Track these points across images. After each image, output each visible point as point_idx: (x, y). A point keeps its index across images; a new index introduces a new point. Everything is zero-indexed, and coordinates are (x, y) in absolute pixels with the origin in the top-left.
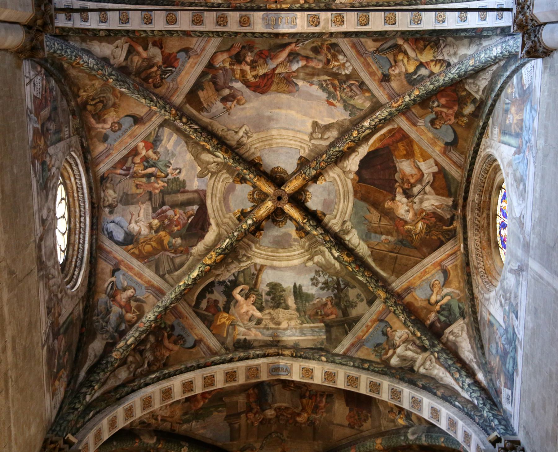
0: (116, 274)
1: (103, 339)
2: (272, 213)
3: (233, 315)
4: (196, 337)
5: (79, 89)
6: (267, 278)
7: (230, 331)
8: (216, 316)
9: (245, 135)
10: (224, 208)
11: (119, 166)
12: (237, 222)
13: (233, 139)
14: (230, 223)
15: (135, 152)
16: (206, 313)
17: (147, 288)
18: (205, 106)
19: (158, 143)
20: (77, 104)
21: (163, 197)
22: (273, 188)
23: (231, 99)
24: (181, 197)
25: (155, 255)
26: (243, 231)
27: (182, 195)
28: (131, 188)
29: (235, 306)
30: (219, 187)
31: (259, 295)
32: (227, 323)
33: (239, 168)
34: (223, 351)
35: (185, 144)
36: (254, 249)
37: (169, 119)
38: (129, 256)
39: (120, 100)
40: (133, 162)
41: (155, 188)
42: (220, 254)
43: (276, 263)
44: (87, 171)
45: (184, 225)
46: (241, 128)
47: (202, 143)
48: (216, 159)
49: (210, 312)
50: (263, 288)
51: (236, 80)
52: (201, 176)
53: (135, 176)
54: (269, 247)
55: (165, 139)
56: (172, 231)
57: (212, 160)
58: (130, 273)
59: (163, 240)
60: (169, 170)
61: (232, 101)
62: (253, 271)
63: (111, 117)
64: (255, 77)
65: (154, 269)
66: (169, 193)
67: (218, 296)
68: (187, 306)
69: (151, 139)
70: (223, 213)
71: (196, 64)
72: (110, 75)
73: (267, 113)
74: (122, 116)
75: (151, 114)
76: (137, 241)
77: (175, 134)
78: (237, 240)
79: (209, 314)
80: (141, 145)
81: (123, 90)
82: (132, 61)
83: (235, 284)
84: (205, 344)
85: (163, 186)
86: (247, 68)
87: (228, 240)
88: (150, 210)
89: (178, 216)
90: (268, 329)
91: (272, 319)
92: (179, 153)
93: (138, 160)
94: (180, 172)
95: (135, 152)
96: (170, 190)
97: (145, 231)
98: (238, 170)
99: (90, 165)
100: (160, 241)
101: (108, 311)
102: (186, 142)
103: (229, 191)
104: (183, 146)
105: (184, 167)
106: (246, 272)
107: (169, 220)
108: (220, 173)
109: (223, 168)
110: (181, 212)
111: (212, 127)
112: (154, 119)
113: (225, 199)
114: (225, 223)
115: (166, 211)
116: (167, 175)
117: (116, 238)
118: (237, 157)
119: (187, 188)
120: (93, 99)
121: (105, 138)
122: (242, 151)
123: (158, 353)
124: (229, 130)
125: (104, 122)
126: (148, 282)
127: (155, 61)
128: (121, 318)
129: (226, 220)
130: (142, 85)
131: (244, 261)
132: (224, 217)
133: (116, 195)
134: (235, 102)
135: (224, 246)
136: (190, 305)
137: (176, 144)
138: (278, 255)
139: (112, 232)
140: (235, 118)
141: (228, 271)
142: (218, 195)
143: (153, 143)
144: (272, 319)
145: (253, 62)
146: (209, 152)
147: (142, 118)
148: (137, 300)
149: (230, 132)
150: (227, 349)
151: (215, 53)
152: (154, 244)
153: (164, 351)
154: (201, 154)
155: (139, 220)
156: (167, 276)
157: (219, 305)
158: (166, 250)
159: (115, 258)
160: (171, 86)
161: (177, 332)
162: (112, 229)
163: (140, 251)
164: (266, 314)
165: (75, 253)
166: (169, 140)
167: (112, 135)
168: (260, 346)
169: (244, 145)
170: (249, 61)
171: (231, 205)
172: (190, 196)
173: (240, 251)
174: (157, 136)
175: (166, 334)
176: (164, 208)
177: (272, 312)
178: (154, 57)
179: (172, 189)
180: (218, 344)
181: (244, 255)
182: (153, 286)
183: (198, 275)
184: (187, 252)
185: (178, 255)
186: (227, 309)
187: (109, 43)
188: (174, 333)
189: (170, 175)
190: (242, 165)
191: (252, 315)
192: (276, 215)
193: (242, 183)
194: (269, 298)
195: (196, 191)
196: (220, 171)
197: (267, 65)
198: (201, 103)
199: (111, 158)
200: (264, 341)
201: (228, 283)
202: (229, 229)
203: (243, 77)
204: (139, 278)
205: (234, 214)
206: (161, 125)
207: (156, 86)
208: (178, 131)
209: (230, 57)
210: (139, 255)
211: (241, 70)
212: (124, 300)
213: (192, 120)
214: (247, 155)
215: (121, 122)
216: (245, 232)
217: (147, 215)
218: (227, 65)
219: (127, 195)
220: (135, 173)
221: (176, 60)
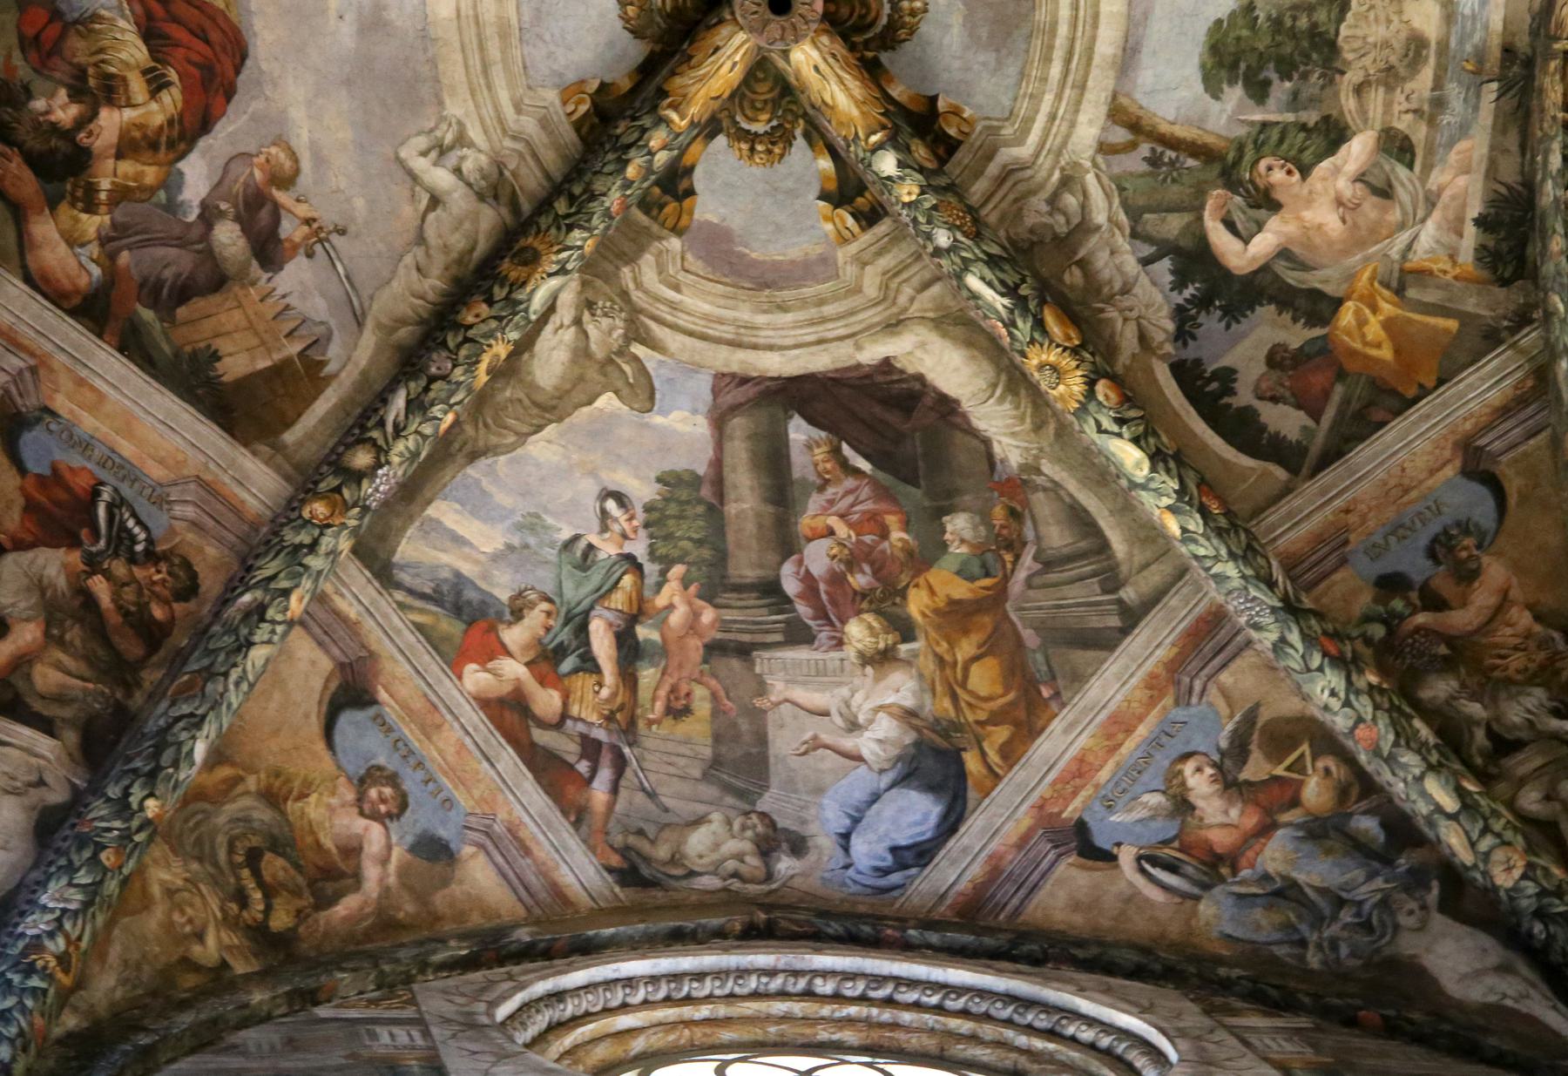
0: (1102, 841)
2: (852, 48)
3: (1351, 277)
4: (1449, 472)
5: (187, 964)
6: (1176, 92)
7: (1431, 296)
8: (1352, 366)
9: (452, 159)
10: (807, 291)
11: (571, 790)
12: (883, 227)
13: (467, 224)
14: (887, 262)
15: (509, 713)
16: (1329, 414)
17: (1183, 700)
18: (294, 349)
19: (470, 594)
20: (264, 976)
21: (739, 588)
22: (725, 31)
23: (264, 215)
24: (745, 499)
25: (1019, 642)
26: (930, 200)
27: (731, 495)
28: (687, 742)
29: (1305, 267)
30: (707, 308)
31: (1263, 138)
32: (1387, 309)
33: (613, 200)
34: (1530, 338)
35: (483, 463)
36: (1024, 152)
37: (355, 532)
38: (1019, 775)
39: (252, 770)
40: (558, 725)
41: (693, 625)
42: (1039, 324)
43: (1107, 43)
44: (588, 949)
45: (882, 493)
46: (413, 177)
47: (482, 376)
48: (565, 314)
49: (1326, 395)
50: (1226, 115)
51: (171, 183)
52: (644, 394)
53: (625, 718)
54: (1022, 75)
55: (449, 560)
56: (910, 553)
57: (569, 335)
58: (1104, 775)
59: (953, 603)
60: (608, 549)
61: (276, 209)
62: (1134, 163)
63: (331, 816)
64: (157, 85)
66: (721, 558)
67: (1248, 347)
68: (1284, 507)
69: (451, 627)
70: (836, 298)
71: (81, 382)
73: (345, 35)
74: (327, 763)
75: (324, 622)
76: (947, 729)
77: (431, 511)
78: (977, 237)
79: (1339, 391)
80: (475, 677)
81: (200, 750)
82: (60, 699)
83: (1194, 260)
84: (1487, 428)
85: (685, 583)
86: (110, 122)
87: (973, 282)
88: (801, 654)
89: (833, 521)
90: (1439, 103)
91: (1390, 77)
92: (525, 494)
93: (547, 701)
94: (620, 498)
96: (706, 553)
97: (901, 689)
98: (626, 208)
99: (562, 937)
100: (956, 616)
102: (473, 457)
103: (725, 259)
104: (491, 472)
105: (593, 473)
106: (1141, 201)
107: (852, 563)
108: (636, 296)
109: (610, 278)
110: (815, 502)
111: (402, 322)
112: (352, 611)
113: (764, 281)
114: (885, 287)
115: (808, 580)
116: (630, 558)
117: (927, 830)
118: (561, 206)
119: (702, 470)
120: (242, 899)
121: (433, 850)
122: (531, 181)
123: (1516, 662)
124: (421, 239)
125: (352, 850)
126: (1155, 687)
127: (62, 583)
129: (871, 289)
130: (181, 657)
131: (1084, 207)
132: (858, 290)
133: (716, 817)
134: (281, 196)
135: (1000, 302)
136: (1287, 490)
137: (479, 506)
138: (1063, 30)
139: (894, 850)
140: (359, 203)
141: (1126, 290)
142: (745, 314)
143: (467, 620)
144: (1390, 77)
145: (78, 92)
146: (524, 346)
147: (341, 666)
148: (1239, 749)
149: (430, 232)
150: (1522, 319)
151: (28, 279)
152: (966, 648)
153: (1505, 635)
154: (533, 387)
155: (843, 711)
156: (1129, 594)
157: (1295, 344)
158: (1000, 594)
159: (1023, 842)
160: (190, 512)
161: (1417, 567)
162: (881, 849)
163: (995, 719)
164: (1363, 112)
165: (988, 1031)
166: (458, 540)
167: (420, 818)
168: (1523, 148)
169: (500, 166)
170: (74, 110)
171: (794, 253)
172: (739, 452)
173: (1030, 220)
174: (435, 598)
175: (1421, 618)
176: (791, 586)
177: (1353, 77)
178: (40, 586)
179: (699, 543)
180: (1492, 363)
181: (1053, 200)
182: (1175, 667)
183: (1136, 441)
184: (1016, 490)
185: (1029, 533)
186: (1318, 307)
188: (1417, 578)
189: (628, 548)
190: (598, 186)
191: (1360, 178)
192: (862, 28)
193: (690, 192)
194: (1281, 89)
195: (719, 421)
196: (625, 294)
197: (95, 17)
198: (279, 371)
199: (530, 830)
200: (1500, 128)
201: (1189, 291)
202: (918, 273)
203: (154, 146)
204: (1129, 731)
205: (844, 241)
206: (384, 573)
207: (189, 589)
208: (412, 492)
209: (53, 204)
210: (1017, 724)
211: (119, 156)
212: (1234, 813)
213: (362, 422)
214: (550, 158)
215: (357, 768)
216: (937, 190)
217: (821, 671)
218: (92, 224)
219: (716, 763)
220: (610, 718)
221: (56, 477)
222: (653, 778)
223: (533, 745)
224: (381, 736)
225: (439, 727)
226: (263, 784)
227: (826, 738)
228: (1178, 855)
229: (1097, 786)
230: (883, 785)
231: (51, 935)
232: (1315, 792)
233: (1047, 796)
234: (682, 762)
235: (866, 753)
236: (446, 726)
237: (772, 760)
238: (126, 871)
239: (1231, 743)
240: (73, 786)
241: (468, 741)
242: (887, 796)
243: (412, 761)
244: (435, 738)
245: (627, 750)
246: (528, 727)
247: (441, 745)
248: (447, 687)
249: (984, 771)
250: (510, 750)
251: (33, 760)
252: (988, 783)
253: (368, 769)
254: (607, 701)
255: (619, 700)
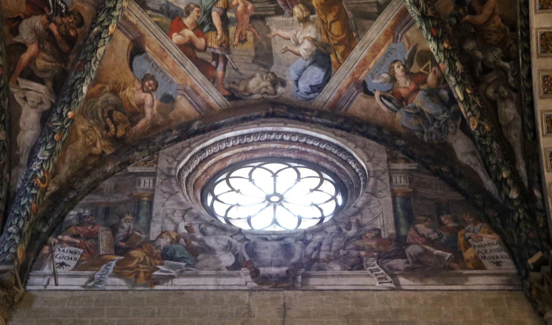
1: (454, 134)
15: (188, 48)
28: (246, 51)
53: (226, 45)
58: (371, 66)
65: (370, 22)
72: (61, 117)
76: (326, 46)
93: (200, 42)
95: (188, 48)
101: (419, 113)
128: (432, 94)
163: (340, 43)
187: (20, 115)
204: (379, 50)
210: (346, 45)
212: (408, 83)
215: (140, 76)
220: (221, 46)
222: (236, 64)
223: (197, 58)
224: (148, 63)
225: (166, 57)
226: (111, 88)
227: (290, 48)
228: (391, 96)
229: (369, 69)
230: (307, 65)
231: (39, 171)
232: (431, 78)
233: (355, 71)
234: (245, 58)
235: (301, 53)
236: (168, 56)
237: (274, 55)
238: (63, 139)
239: (409, 58)
240: (51, 102)
241: (176, 60)
242: (308, 68)
243: (159, 70)
244: (165, 61)
245: (227, 56)
246: (195, 52)
247: (167, 63)
248: (168, 43)
249: (337, 62)
250: (190, 61)
251: (39, 95)
252: (338, 65)
253: (145, 76)
254: (220, 40)
255: (223, 39)
